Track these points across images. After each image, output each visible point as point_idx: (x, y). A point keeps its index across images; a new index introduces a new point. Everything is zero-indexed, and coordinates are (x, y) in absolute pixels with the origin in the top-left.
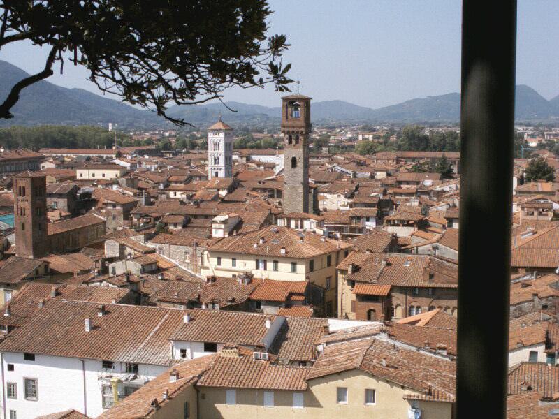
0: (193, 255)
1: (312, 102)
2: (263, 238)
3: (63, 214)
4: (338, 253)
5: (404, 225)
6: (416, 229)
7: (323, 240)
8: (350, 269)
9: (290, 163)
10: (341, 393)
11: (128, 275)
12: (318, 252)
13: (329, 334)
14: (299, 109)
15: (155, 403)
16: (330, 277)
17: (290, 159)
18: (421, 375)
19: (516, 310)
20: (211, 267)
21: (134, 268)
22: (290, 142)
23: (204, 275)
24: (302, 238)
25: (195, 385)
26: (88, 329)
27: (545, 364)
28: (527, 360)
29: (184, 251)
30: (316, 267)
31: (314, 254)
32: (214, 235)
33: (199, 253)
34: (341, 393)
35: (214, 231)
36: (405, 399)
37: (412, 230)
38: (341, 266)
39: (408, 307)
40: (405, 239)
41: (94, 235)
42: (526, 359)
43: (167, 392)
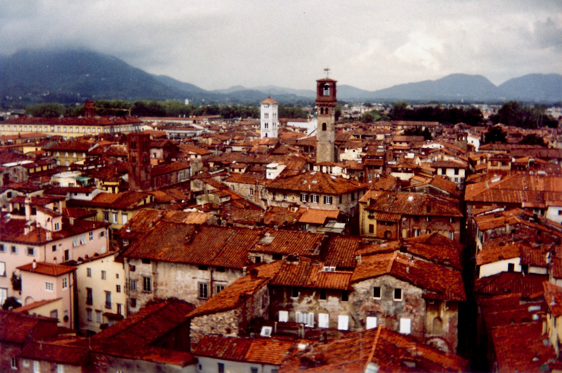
0: (256, 191)
1: (338, 84)
3: (161, 161)
5: (404, 172)
6: (413, 174)
9: (321, 127)
14: (329, 89)
17: (321, 124)
19: (492, 233)
22: (322, 113)
27: (520, 273)
29: (249, 187)
32: (268, 177)
38: (362, 199)
39: (411, 230)
42: (506, 269)
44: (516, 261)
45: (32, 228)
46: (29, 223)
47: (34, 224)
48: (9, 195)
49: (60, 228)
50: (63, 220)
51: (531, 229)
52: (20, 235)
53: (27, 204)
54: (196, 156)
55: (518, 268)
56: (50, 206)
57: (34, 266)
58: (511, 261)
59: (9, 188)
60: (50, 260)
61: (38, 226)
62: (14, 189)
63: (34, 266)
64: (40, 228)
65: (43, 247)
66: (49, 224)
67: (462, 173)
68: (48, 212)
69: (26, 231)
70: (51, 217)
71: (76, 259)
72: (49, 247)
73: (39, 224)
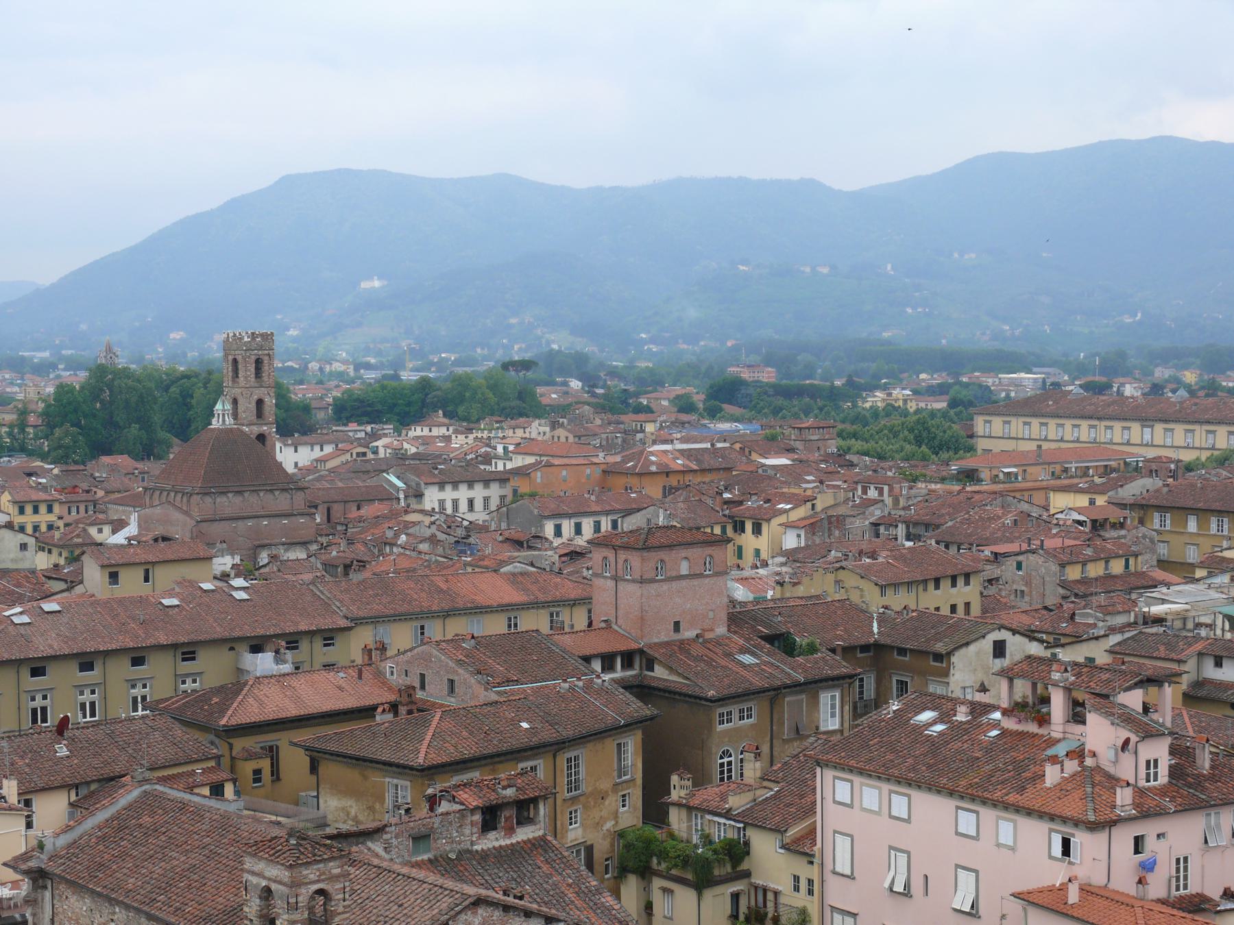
45: (1071, 766)
46: (1060, 750)
47: (1078, 754)
48: (999, 649)
49: (1163, 778)
50: (1173, 751)
52: (1030, 790)
53: (1055, 685)
56: (1133, 699)
57: (1073, 896)
59: (1001, 627)
60: (1124, 882)
61: (1089, 762)
62: (1014, 632)
63: (1073, 896)
64: (1098, 769)
65: (1102, 837)
66: (1127, 759)
68: (1126, 718)
69: (1052, 774)
70: (1134, 738)
71: (1215, 893)
72: (1123, 838)
73: (1094, 755)
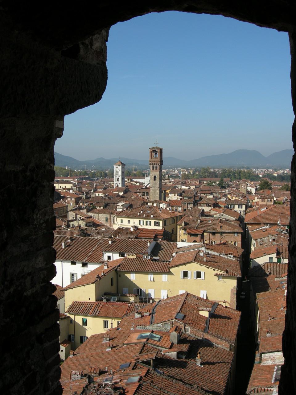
2: (142, 211)
4: (177, 217)
7: (170, 211)
8: (183, 224)
10: (185, 274)
11: (80, 226)
12: (169, 217)
13: (177, 249)
15: (98, 276)
16: (174, 229)
18: (222, 265)
19: (261, 241)
20: (119, 223)
21: (82, 224)
22: (153, 169)
23: (115, 227)
24: (160, 211)
25: (116, 270)
26: (63, 247)
28: (268, 261)
29: (105, 217)
30: (167, 223)
31: (167, 218)
33: (112, 218)
34: (185, 274)
35: (118, 209)
36: (215, 276)
37: (210, 208)
40: (207, 212)
41: (62, 212)
43: (104, 272)
44: (274, 256)
51: (284, 238)
54: (71, 199)
55: (275, 260)
58: (271, 256)
67: (244, 207)
